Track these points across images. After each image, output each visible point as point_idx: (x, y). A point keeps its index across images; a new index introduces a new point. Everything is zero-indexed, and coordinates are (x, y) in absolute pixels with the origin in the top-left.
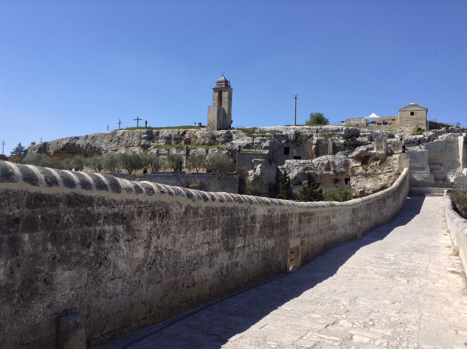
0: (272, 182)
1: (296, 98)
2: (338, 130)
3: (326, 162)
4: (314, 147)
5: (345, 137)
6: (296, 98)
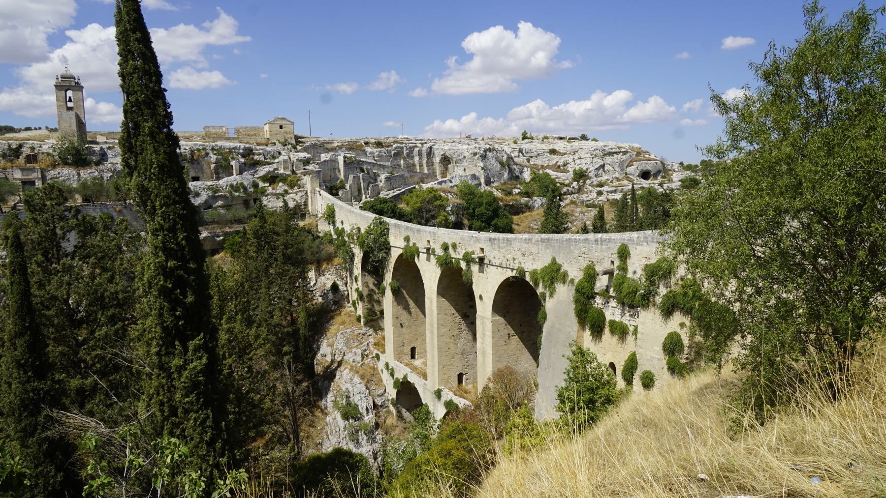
2: (235, 148)
3: (235, 183)
4: (213, 166)
5: (243, 156)
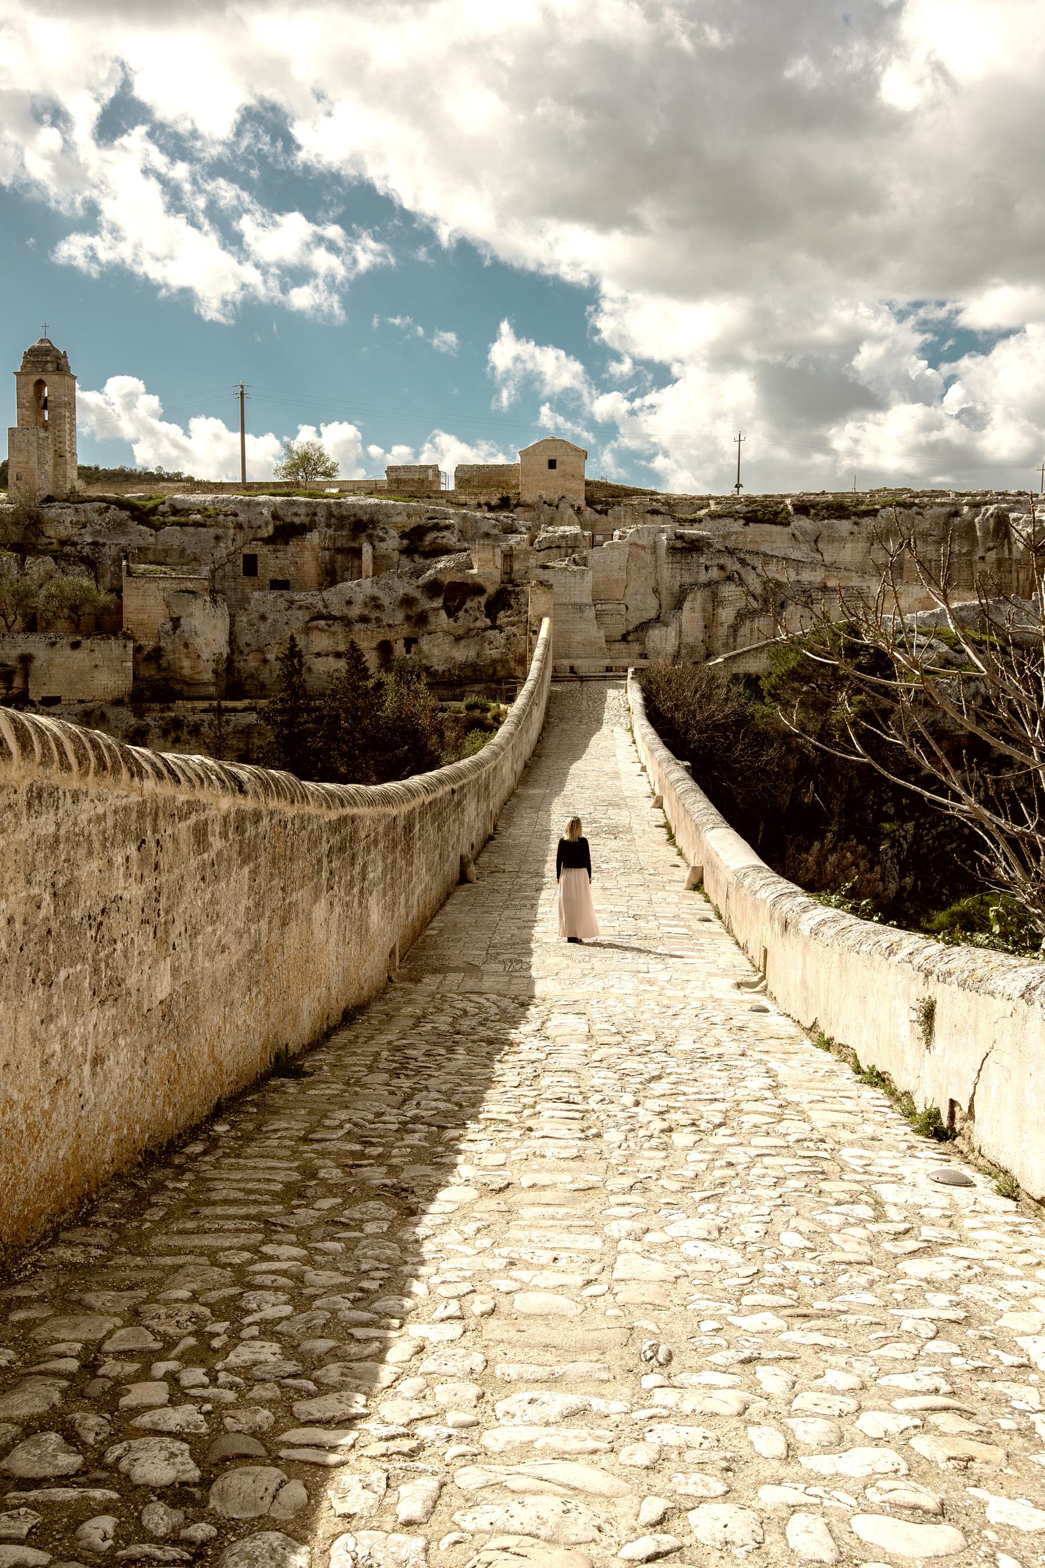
0: (221, 654)
1: (242, 394)
6: (242, 394)
